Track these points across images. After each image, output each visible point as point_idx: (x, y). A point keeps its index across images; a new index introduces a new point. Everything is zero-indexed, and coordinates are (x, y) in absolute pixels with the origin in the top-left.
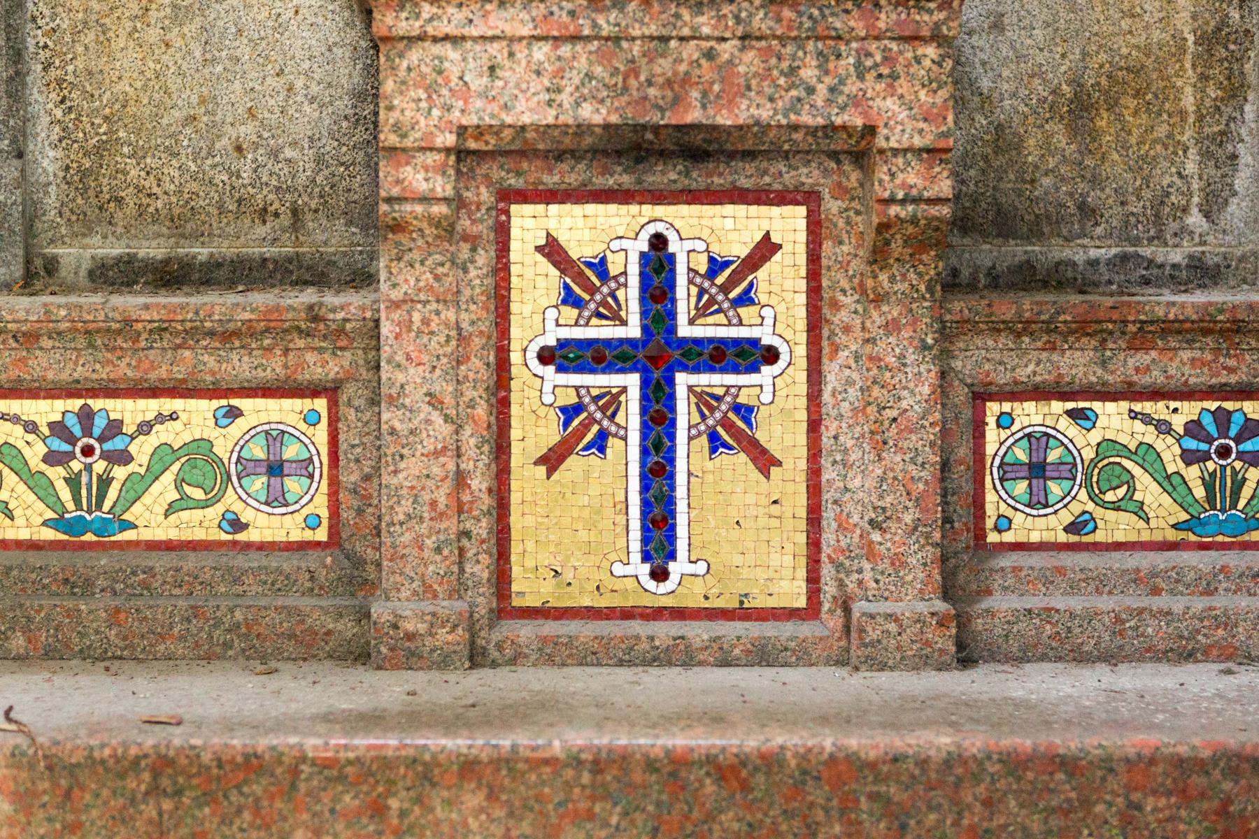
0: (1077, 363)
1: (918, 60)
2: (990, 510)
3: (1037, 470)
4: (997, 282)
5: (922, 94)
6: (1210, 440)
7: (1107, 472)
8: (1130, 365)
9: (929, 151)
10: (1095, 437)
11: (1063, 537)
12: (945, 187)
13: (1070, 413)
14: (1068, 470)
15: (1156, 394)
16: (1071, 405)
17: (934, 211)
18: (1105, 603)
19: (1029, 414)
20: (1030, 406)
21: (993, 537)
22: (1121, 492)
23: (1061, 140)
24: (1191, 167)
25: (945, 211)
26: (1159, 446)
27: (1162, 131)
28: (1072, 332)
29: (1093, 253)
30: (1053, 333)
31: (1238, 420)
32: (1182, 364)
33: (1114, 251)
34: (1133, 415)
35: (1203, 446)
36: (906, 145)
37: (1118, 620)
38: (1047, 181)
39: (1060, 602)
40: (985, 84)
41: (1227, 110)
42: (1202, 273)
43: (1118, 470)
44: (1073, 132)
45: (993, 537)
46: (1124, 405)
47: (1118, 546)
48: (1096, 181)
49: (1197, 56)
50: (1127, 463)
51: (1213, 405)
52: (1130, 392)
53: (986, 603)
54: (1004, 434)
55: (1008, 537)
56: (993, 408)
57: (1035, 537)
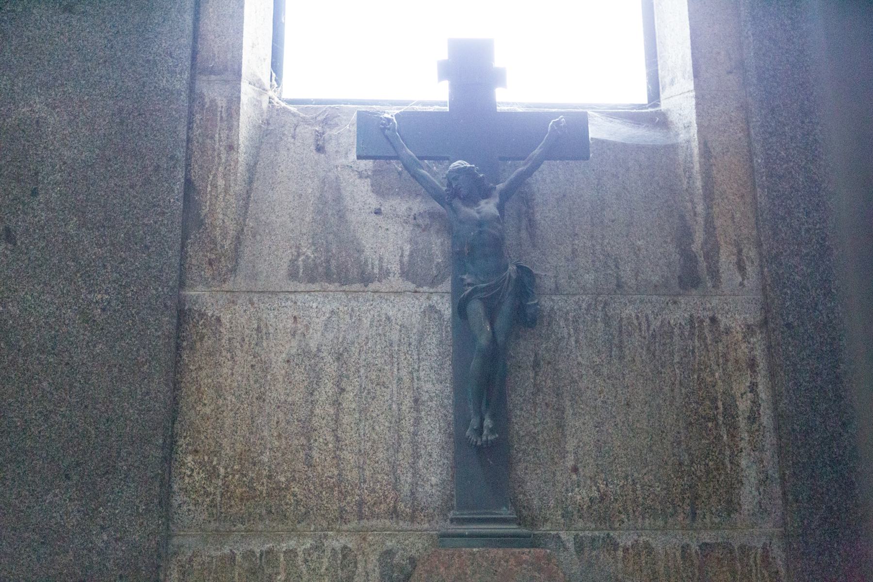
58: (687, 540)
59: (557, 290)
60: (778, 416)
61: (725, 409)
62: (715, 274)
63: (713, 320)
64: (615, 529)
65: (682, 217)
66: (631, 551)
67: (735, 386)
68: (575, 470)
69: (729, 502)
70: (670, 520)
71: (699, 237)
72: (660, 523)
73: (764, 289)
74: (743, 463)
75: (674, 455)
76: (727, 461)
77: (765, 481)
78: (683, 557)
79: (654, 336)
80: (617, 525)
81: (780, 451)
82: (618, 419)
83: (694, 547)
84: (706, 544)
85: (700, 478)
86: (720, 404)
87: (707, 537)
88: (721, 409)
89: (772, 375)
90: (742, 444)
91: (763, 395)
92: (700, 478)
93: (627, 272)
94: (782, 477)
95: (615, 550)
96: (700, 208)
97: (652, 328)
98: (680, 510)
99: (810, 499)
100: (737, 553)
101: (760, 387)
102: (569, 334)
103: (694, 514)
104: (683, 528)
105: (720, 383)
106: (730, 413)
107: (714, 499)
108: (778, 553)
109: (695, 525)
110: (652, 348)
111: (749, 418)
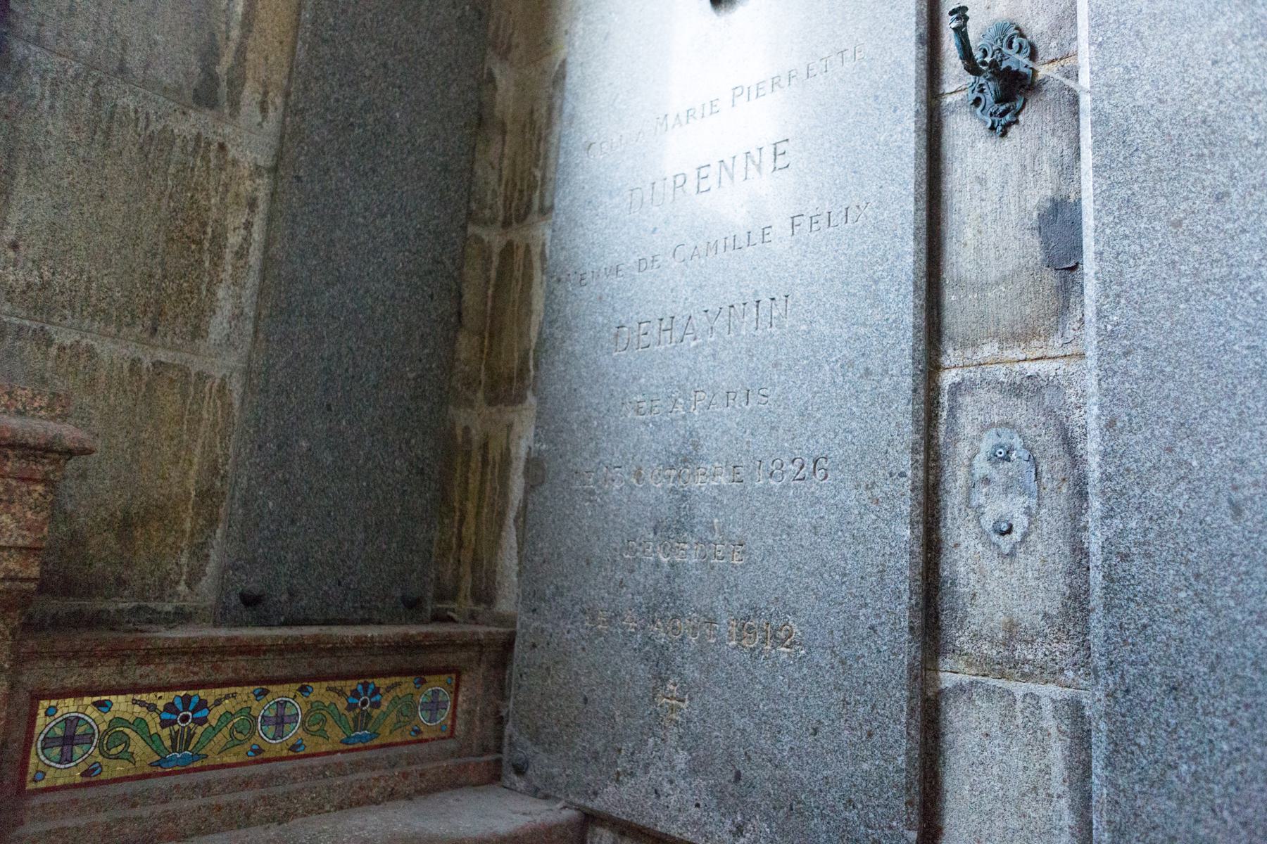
0: (104, 673)
1: (29, 493)
2: (31, 769)
3: (68, 740)
4: (56, 623)
5: (29, 514)
6: (177, 713)
7: (115, 736)
8: (136, 673)
9: (26, 548)
10: (109, 717)
11: (79, 780)
12: (35, 571)
13: (94, 704)
14: (88, 738)
15: (150, 689)
16: (96, 699)
17: (25, 586)
18: (102, 818)
19: (68, 707)
20: (70, 701)
21: (30, 786)
22: (120, 748)
23: (112, 542)
24: (184, 560)
25: (33, 586)
26: (148, 719)
27: (170, 540)
28: (104, 656)
29: (121, 605)
30: (91, 657)
31: (195, 700)
32: (168, 672)
33: (134, 604)
34: (135, 702)
35: (174, 717)
36: (11, 543)
37: (108, 827)
38: (99, 565)
39: (70, 823)
40: (69, 507)
41: (207, 531)
42: (182, 617)
43: (120, 735)
44: (119, 537)
45: (30, 786)
46: (130, 696)
47: (115, 781)
48: (129, 565)
49: (195, 503)
50: (127, 731)
51: (183, 693)
52: (136, 689)
53: (20, 831)
54: (49, 720)
55: (42, 785)
56: (45, 704)
57: (60, 782)
58: (139, 354)
59: (38, 40)
60: (268, 260)
61: (214, 237)
62: (235, 104)
63: (222, 147)
64: (54, 324)
65: (212, 35)
66: (68, 351)
67: (230, 218)
68: (14, 246)
69: (197, 327)
70: (125, 329)
71: (227, 60)
72: (112, 329)
73: (282, 137)
74: (221, 293)
75: (145, 264)
76: (203, 287)
77: (238, 316)
78: (131, 370)
79: (151, 138)
80: (56, 319)
81: (261, 292)
82: (85, 209)
83: (147, 362)
84: (161, 363)
85: (169, 296)
86: (209, 230)
87: (162, 355)
88: (210, 235)
89: (270, 219)
90: (223, 276)
91: (256, 236)
92: (169, 296)
93: (134, 60)
94: (258, 317)
95: (48, 346)
96: (235, 33)
97: (151, 128)
98: (138, 322)
99: (280, 341)
100: (193, 379)
101: (255, 227)
102: (43, 94)
103: (154, 330)
104: (138, 341)
105: (214, 210)
106: (218, 240)
107: (180, 319)
108: (236, 387)
109: (153, 341)
110: (146, 149)
111: (237, 253)
